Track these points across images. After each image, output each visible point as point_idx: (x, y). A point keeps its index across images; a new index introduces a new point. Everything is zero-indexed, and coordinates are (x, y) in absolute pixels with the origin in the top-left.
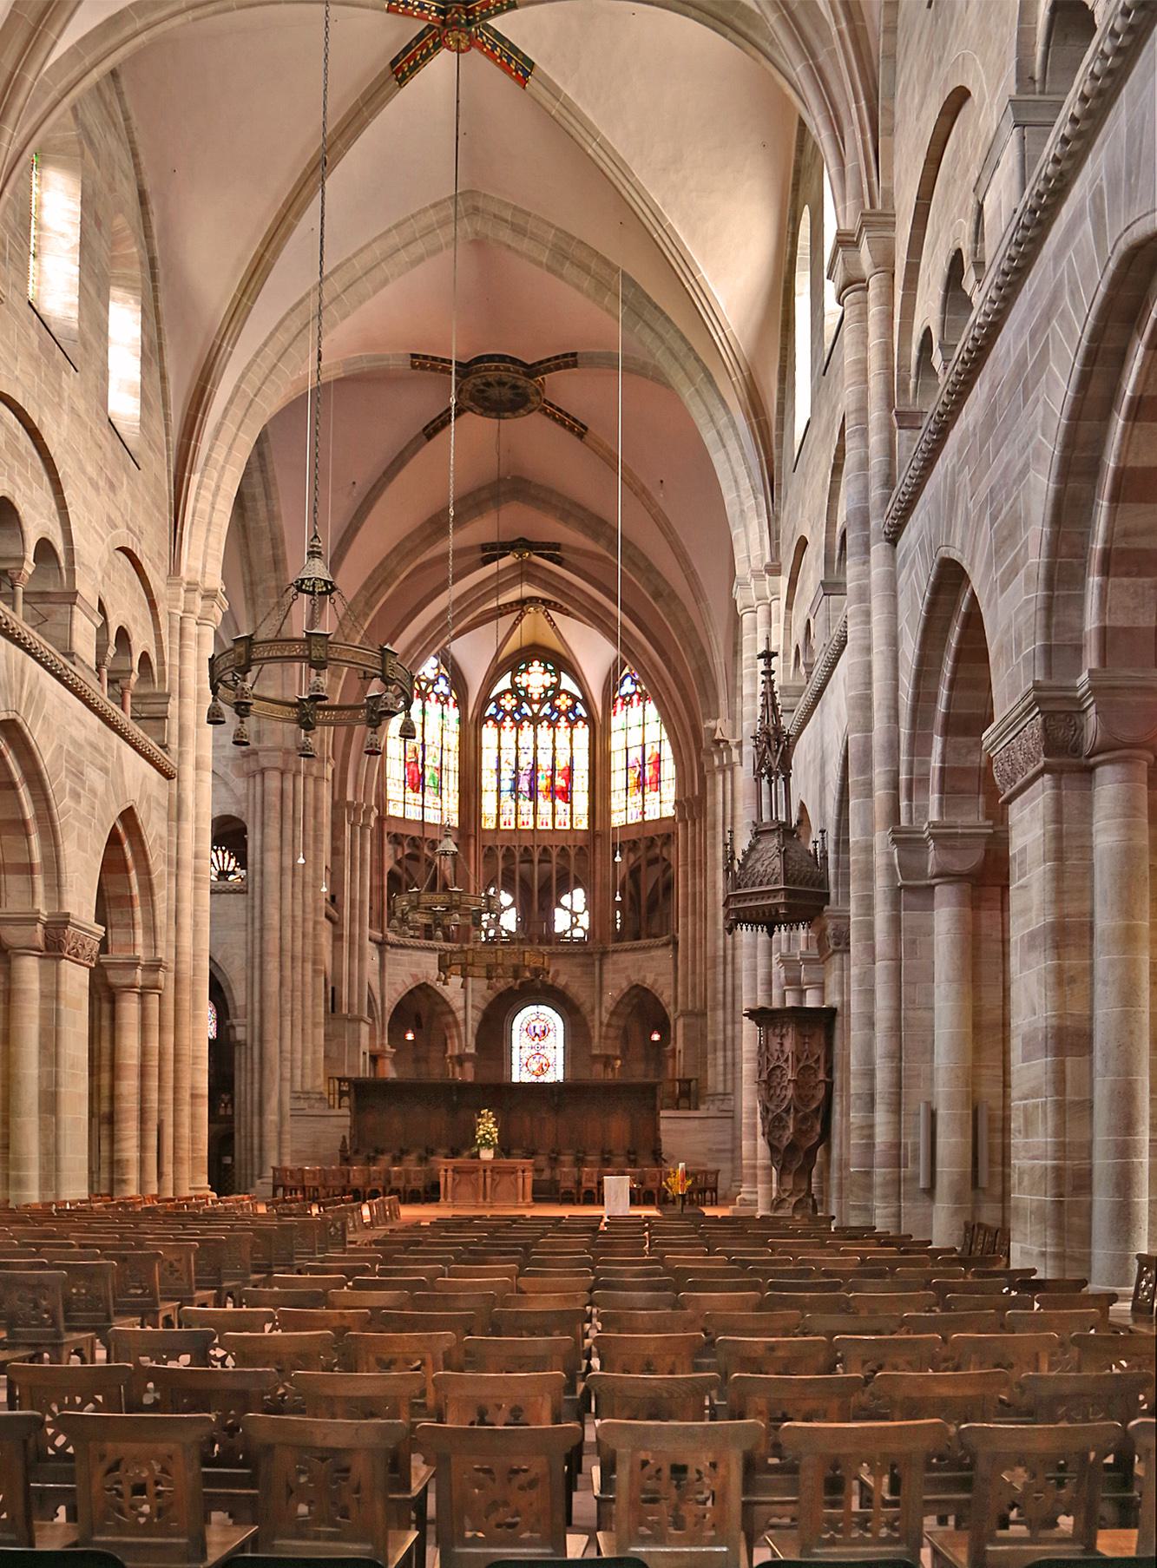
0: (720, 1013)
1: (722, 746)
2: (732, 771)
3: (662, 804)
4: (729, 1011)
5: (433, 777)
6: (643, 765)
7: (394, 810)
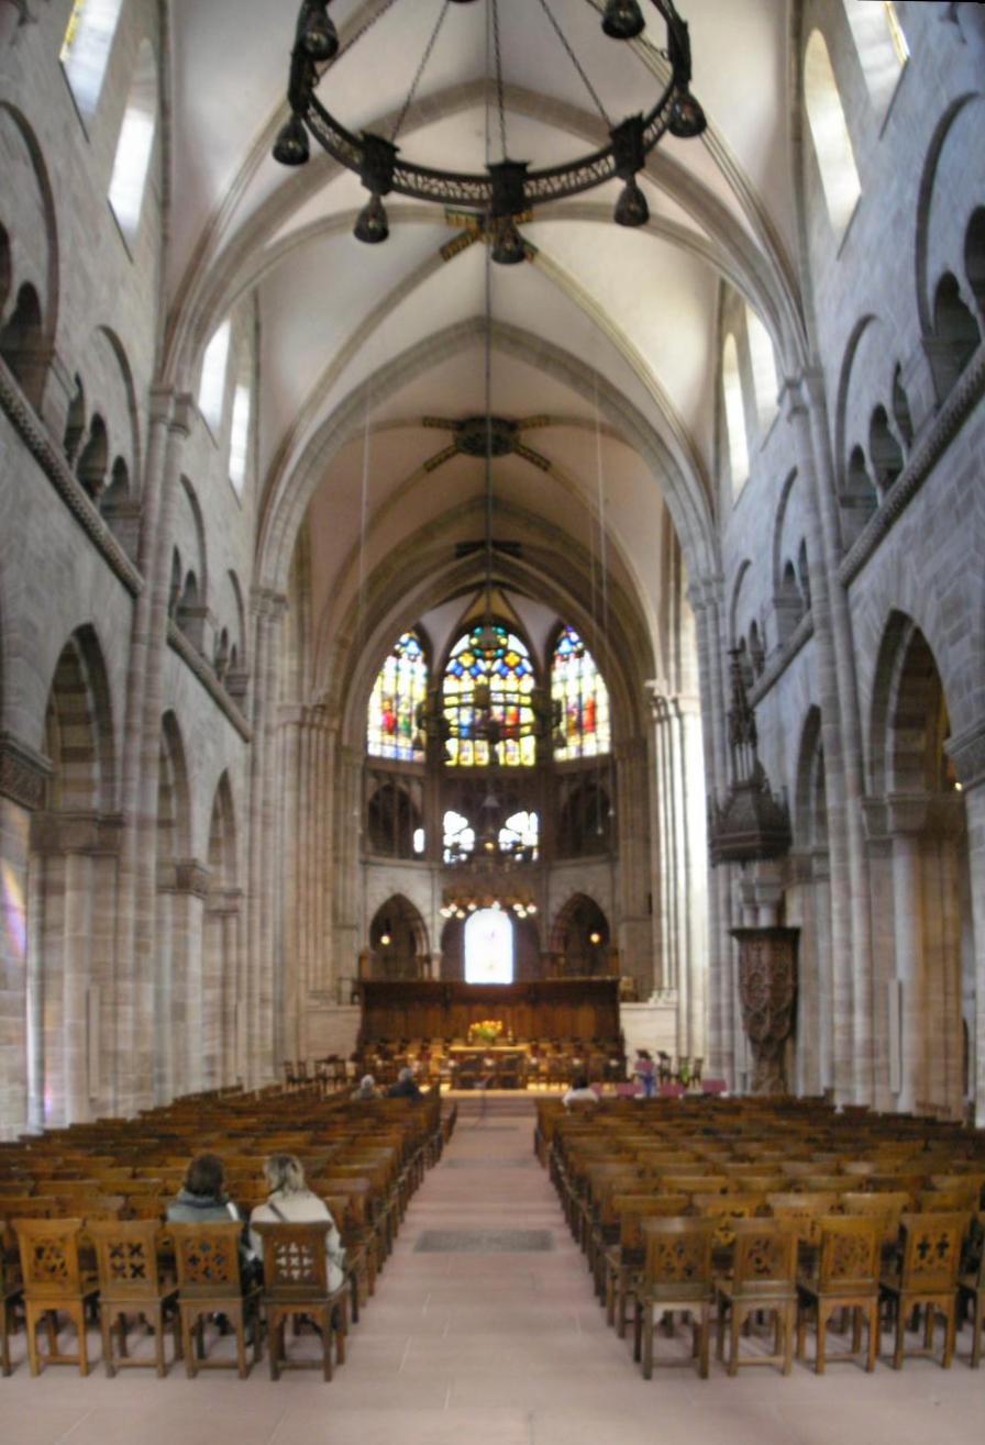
3: (597, 743)
5: (405, 723)
6: (580, 711)
7: (374, 750)
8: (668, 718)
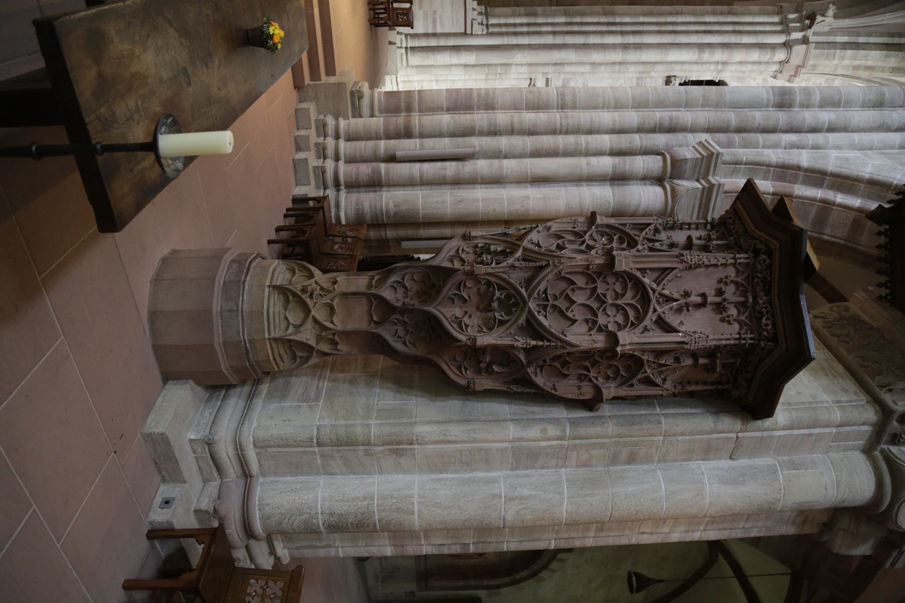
0: (562, 20)
1: (807, 22)
2: (782, 32)
4: (565, 29)
8: (787, 31)
